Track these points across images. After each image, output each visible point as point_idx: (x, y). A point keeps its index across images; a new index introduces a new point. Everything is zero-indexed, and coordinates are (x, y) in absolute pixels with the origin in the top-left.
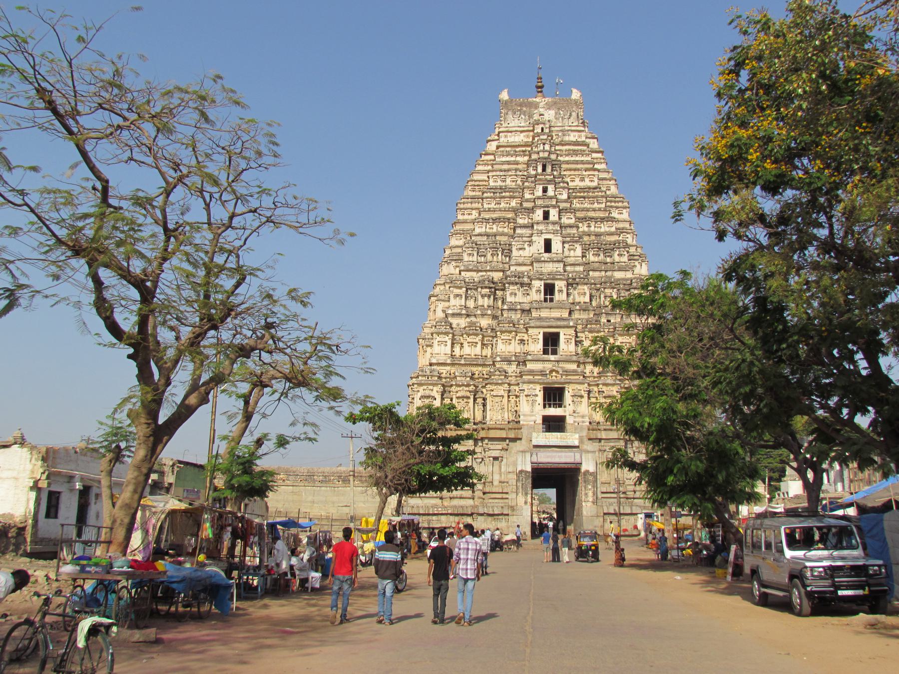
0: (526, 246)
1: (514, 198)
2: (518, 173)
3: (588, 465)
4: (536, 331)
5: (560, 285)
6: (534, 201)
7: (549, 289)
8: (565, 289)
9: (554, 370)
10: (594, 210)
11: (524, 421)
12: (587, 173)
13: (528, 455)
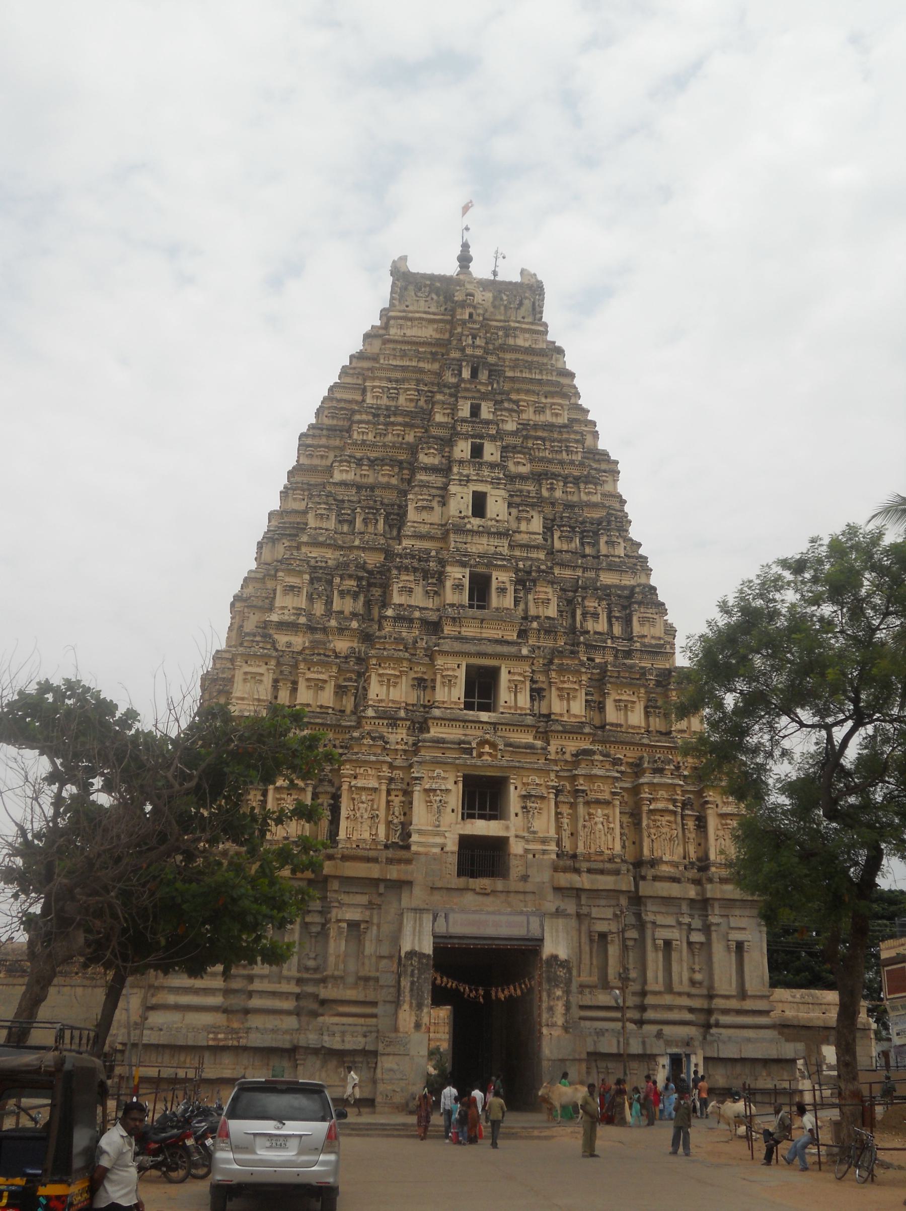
0: (435, 504)
1: (412, 426)
2: (422, 387)
3: (557, 945)
4: (451, 662)
5: (501, 578)
7: (480, 588)
8: (511, 589)
9: (487, 742)
10: (562, 463)
12: (549, 400)
13: (427, 919)
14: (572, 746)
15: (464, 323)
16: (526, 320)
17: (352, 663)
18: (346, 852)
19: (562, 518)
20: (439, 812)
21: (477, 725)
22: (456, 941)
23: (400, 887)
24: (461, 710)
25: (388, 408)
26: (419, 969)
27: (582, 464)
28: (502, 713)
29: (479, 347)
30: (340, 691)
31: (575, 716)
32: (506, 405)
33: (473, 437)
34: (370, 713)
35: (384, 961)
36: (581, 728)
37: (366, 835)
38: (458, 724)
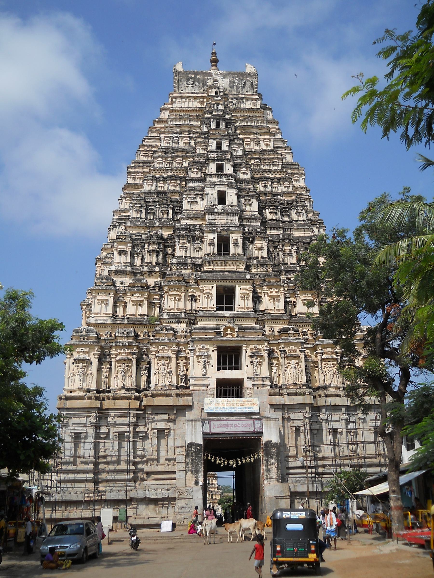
0: (198, 199)
1: (187, 157)
2: (192, 135)
3: (270, 435)
5: (235, 237)
6: (207, 156)
7: (223, 245)
8: (240, 243)
10: (270, 171)
11: (195, 386)
12: (262, 137)
13: (199, 424)
14: (277, 327)
15: (212, 97)
16: (248, 93)
17: (157, 290)
18: (154, 392)
19: (270, 202)
20: (205, 367)
21: (224, 319)
22: (215, 436)
23: (185, 409)
24: (215, 311)
25: (173, 148)
26: (195, 452)
27: (281, 171)
28: (238, 311)
29: (220, 110)
30: (151, 305)
31: (279, 310)
32: (236, 141)
33: (217, 160)
34: (165, 316)
35: (179, 449)
36: (282, 316)
37: (167, 383)
38: (213, 319)
